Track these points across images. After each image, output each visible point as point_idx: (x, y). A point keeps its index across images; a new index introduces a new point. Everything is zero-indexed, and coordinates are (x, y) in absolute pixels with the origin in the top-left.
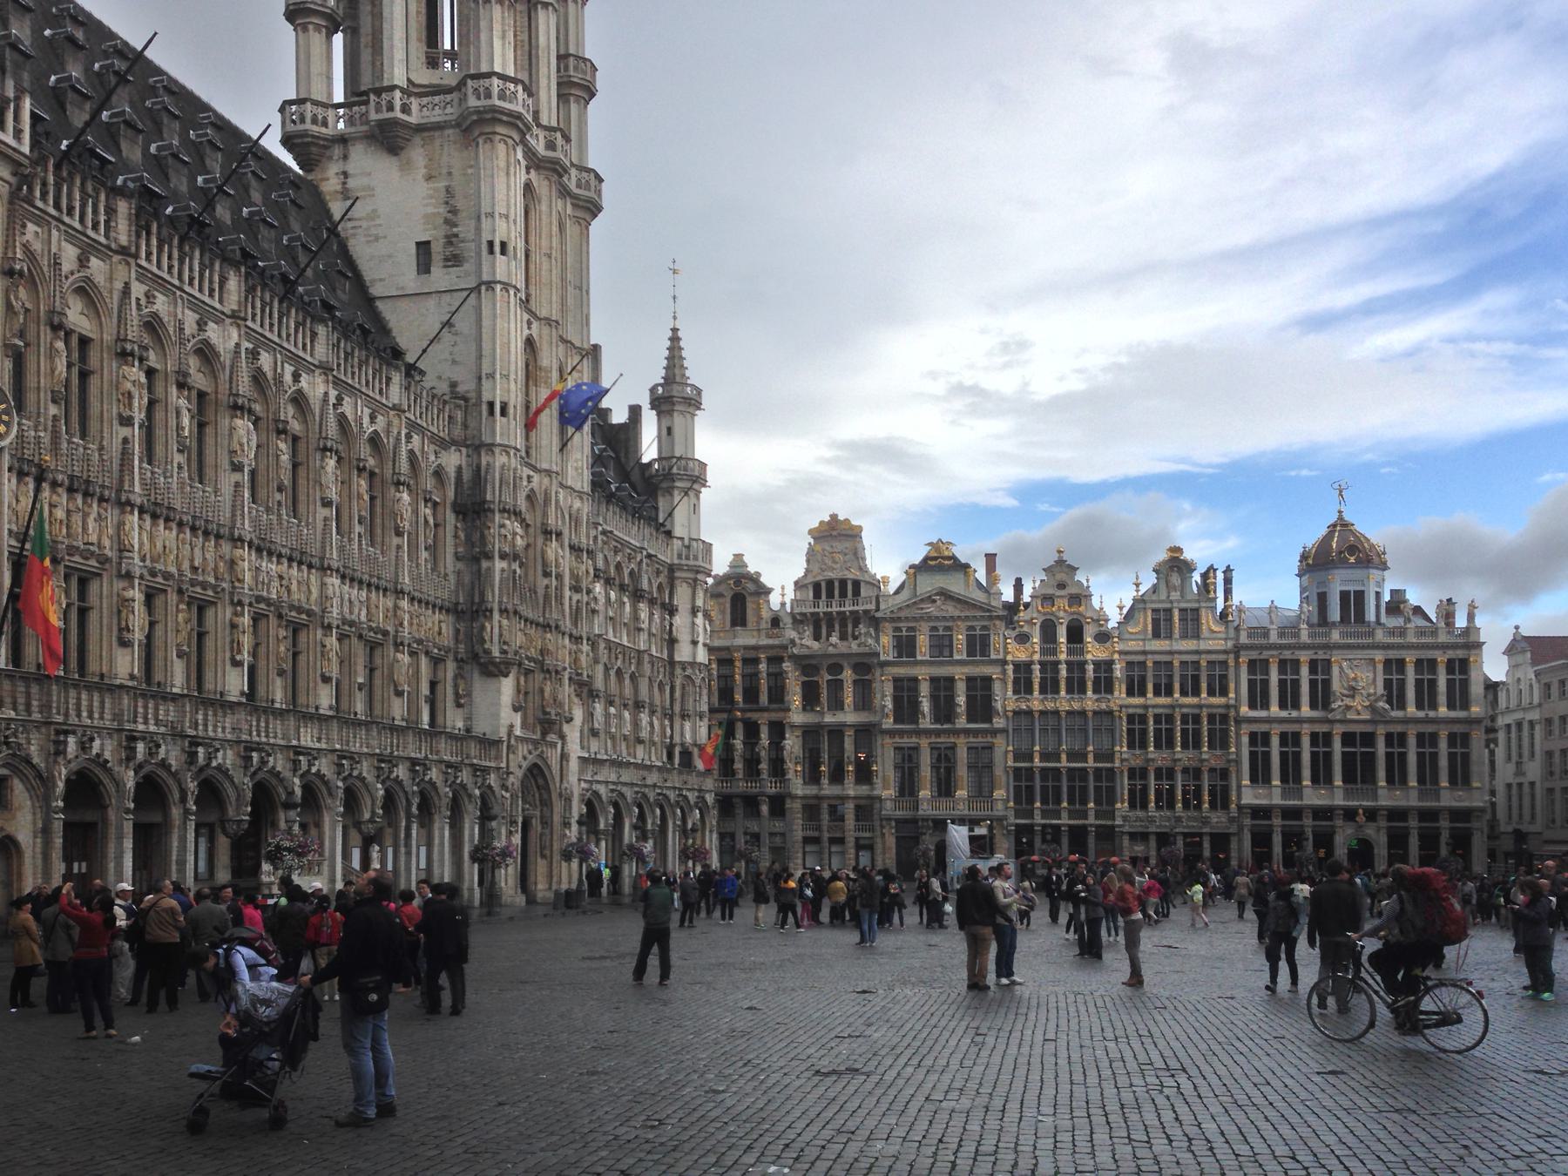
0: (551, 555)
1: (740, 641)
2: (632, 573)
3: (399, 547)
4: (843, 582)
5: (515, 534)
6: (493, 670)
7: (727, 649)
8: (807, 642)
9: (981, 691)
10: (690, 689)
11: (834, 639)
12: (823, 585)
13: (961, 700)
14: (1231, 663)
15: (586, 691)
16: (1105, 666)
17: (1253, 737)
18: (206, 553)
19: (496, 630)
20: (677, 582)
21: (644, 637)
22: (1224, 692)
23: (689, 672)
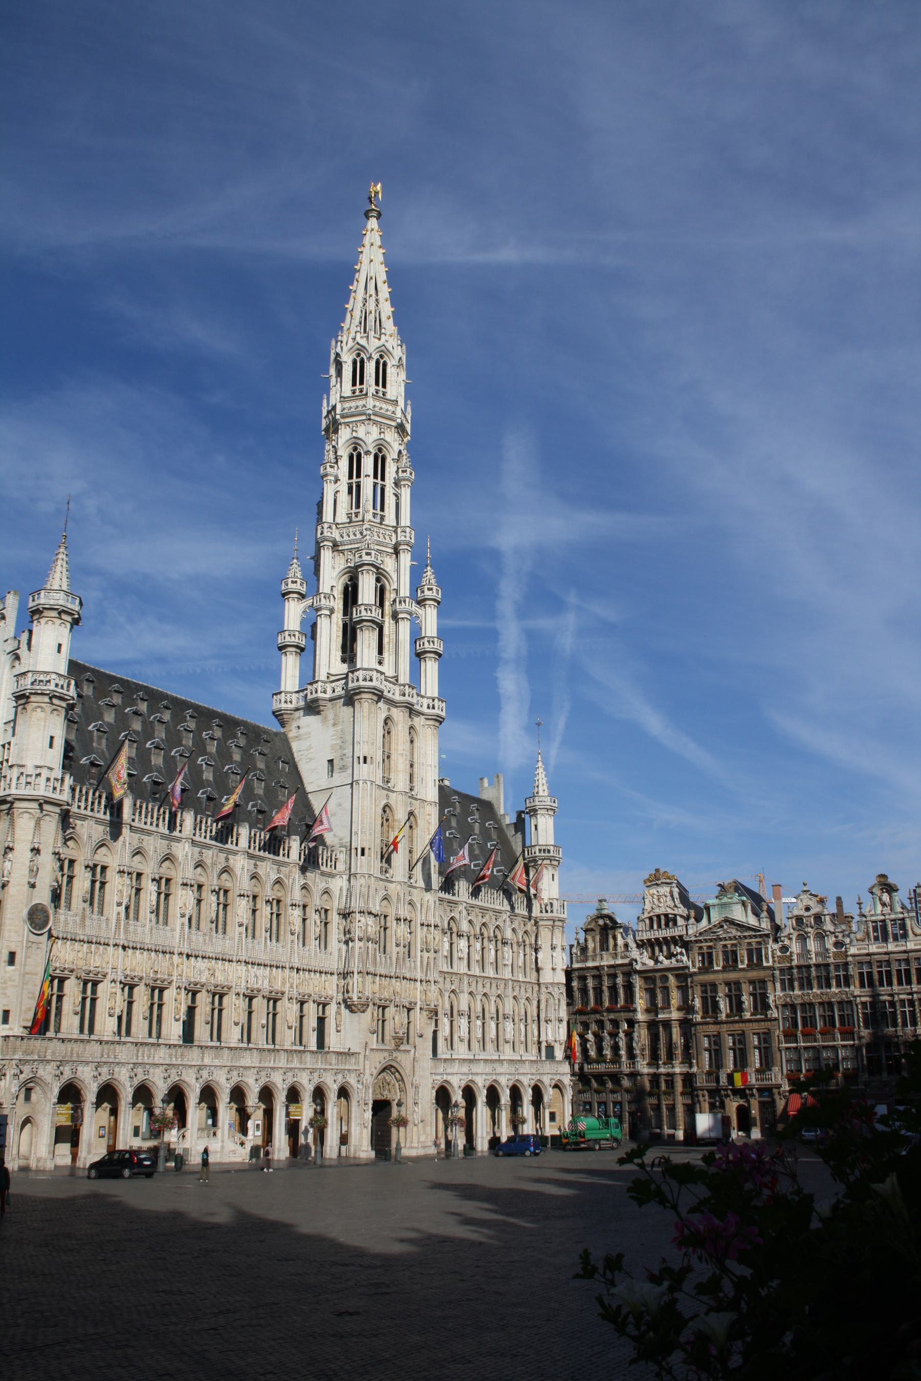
0: (400, 933)
3: (292, 942)
5: (367, 925)
7: (596, 968)
8: (644, 960)
10: (551, 1001)
12: (655, 918)
18: (162, 964)
20: (541, 929)
23: (550, 990)
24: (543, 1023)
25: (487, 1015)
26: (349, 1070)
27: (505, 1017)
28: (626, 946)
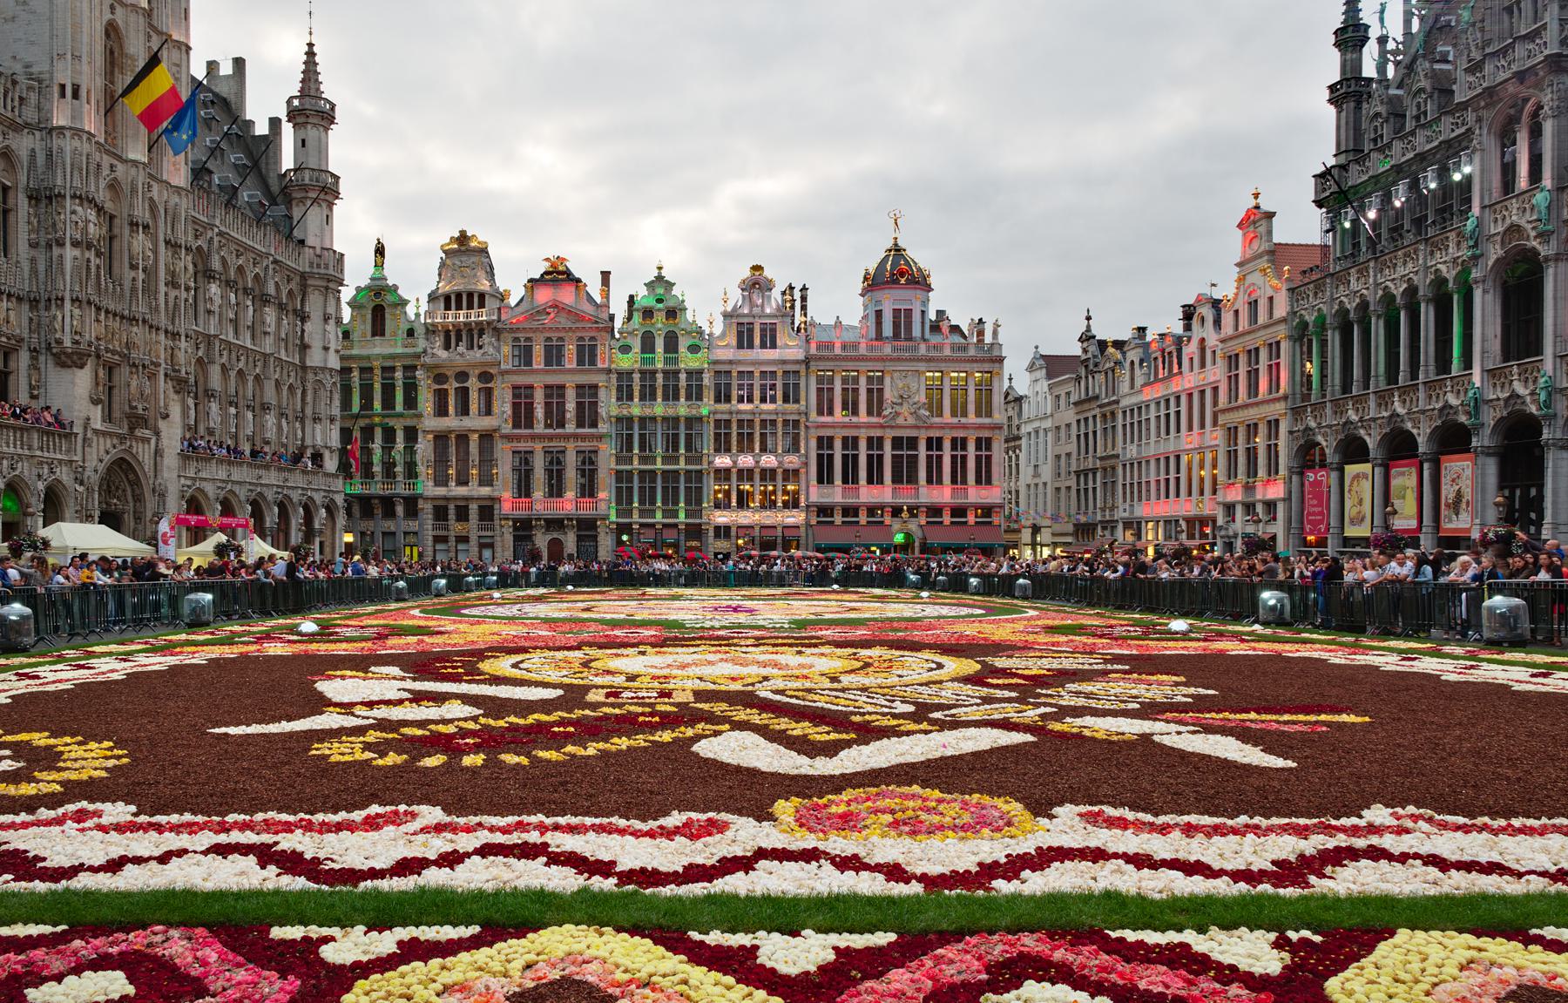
1: (377, 351)
2: (257, 276)
4: (470, 295)
5: (87, 221)
6: (70, 360)
7: (368, 358)
9: (588, 392)
11: (461, 349)
13: (571, 406)
14: (803, 373)
15: (190, 387)
16: (694, 374)
17: (820, 439)
19: (67, 320)
21: (269, 341)
22: (797, 401)
24: (308, 422)
25: (241, 404)
26: (60, 461)
27: (265, 408)
28: (411, 333)
